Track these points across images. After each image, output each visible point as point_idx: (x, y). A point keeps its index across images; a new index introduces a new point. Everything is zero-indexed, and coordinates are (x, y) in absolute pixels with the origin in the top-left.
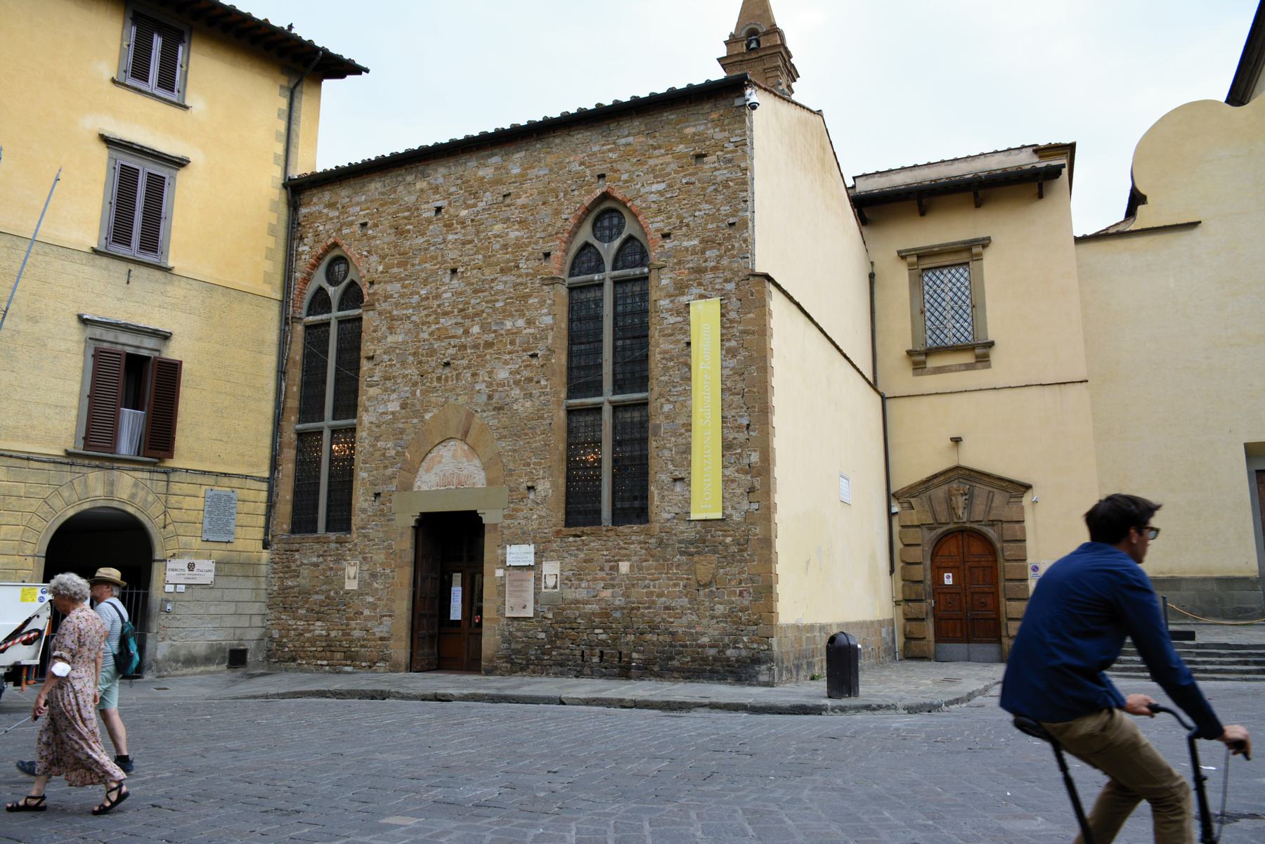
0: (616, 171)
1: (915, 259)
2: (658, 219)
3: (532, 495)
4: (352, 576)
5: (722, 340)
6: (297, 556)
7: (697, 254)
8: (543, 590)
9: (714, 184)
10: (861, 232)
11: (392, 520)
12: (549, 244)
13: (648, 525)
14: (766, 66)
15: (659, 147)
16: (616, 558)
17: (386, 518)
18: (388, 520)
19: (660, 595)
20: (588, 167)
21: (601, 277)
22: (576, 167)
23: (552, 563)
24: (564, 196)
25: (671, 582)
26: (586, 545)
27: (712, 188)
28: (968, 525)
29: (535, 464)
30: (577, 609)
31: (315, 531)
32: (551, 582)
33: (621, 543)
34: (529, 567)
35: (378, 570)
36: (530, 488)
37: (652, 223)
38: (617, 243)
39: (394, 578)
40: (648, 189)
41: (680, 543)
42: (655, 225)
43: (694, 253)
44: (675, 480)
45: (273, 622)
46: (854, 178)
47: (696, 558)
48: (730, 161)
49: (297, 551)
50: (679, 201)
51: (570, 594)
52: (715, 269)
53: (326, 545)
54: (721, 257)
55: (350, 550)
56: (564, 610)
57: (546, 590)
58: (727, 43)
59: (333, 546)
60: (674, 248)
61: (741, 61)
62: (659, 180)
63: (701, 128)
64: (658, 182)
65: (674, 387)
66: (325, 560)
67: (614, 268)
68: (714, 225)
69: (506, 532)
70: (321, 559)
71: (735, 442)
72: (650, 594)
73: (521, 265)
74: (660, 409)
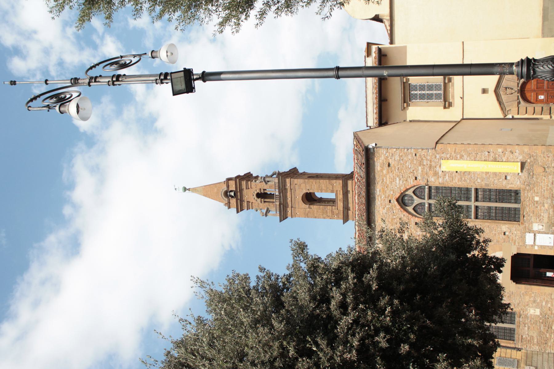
0: (389, 196)
1: (405, 104)
2: (409, 181)
3: (507, 233)
4: (534, 311)
5: (457, 160)
6: (524, 337)
7: (424, 168)
8: (544, 230)
9: (400, 160)
10: (391, 124)
11: (512, 292)
12: (412, 222)
13: (521, 190)
14: (245, 188)
15: (383, 179)
16: (533, 202)
17: (511, 295)
18: (512, 294)
19: (548, 186)
20: (386, 206)
21: (427, 204)
22: (385, 211)
23: (534, 226)
24: (395, 216)
25: (543, 181)
26: (528, 212)
27: (401, 161)
28: (519, 88)
29: (495, 232)
30: (551, 217)
31: (514, 330)
32: (541, 227)
33: (527, 199)
34: (535, 235)
35: (532, 299)
36: (504, 234)
37: (410, 183)
38: (415, 197)
39: (536, 293)
40: (398, 184)
41: (529, 178)
42: (411, 182)
43: (424, 169)
44: (506, 179)
45: (552, 349)
46: (367, 126)
47: (534, 172)
48: (392, 154)
49: (522, 336)
50: (404, 173)
51: (546, 220)
52: (431, 161)
53: (521, 323)
54: (427, 159)
55: (523, 312)
56: (551, 222)
57: (544, 229)
59: (521, 319)
60: (421, 176)
61: (240, 201)
62: (395, 180)
63: (379, 164)
64: (396, 180)
65: (472, 178)
66: (527, 323)
67: (424, 199)
68: (415, 161)
69: (520, 244)
70: (526, 325)
71: (494, 157)
72: (547, 190)
73: (419, 234)
74: (480, 183)
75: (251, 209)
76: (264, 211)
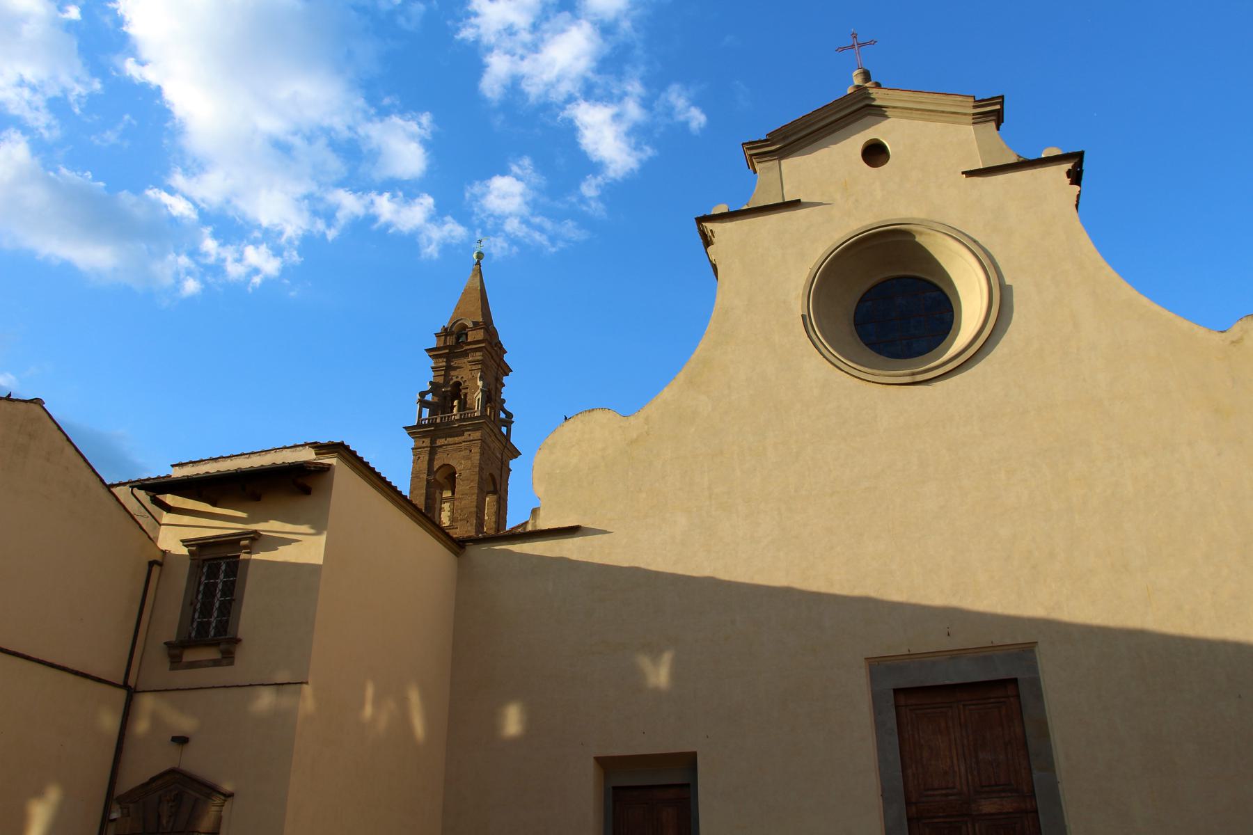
58: (438, 335)
75: (433, 374)
76: (429, 397)
